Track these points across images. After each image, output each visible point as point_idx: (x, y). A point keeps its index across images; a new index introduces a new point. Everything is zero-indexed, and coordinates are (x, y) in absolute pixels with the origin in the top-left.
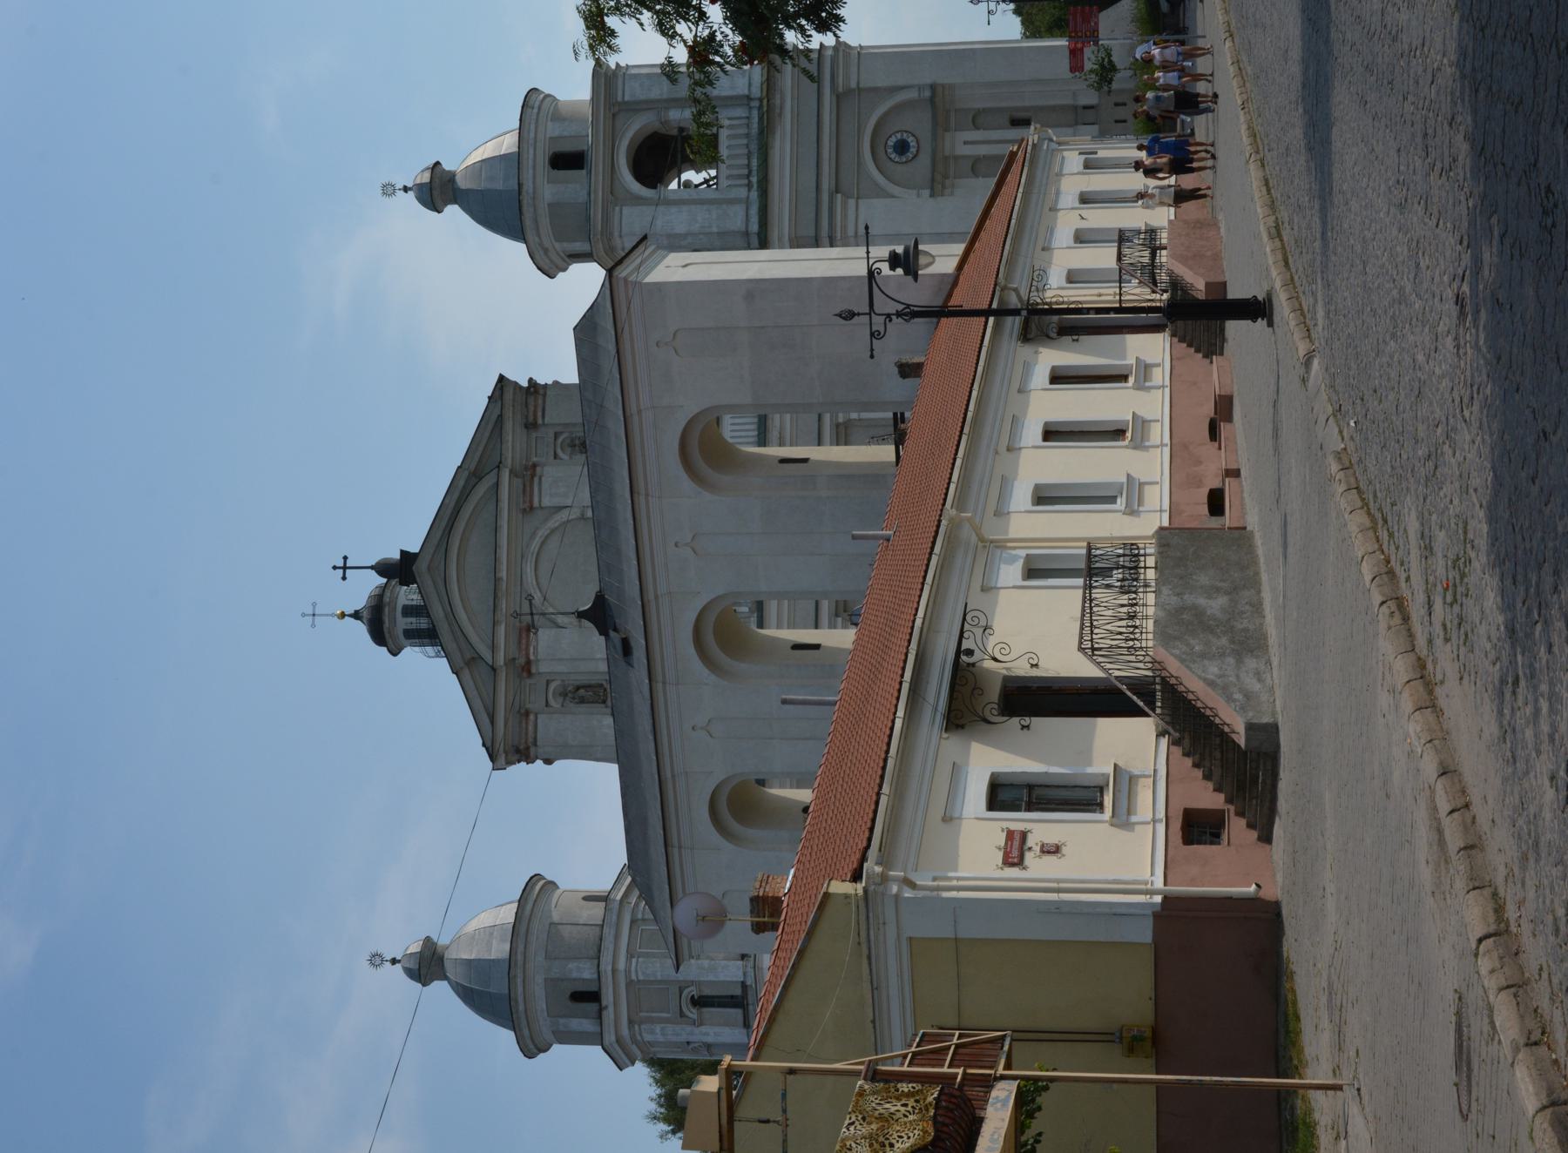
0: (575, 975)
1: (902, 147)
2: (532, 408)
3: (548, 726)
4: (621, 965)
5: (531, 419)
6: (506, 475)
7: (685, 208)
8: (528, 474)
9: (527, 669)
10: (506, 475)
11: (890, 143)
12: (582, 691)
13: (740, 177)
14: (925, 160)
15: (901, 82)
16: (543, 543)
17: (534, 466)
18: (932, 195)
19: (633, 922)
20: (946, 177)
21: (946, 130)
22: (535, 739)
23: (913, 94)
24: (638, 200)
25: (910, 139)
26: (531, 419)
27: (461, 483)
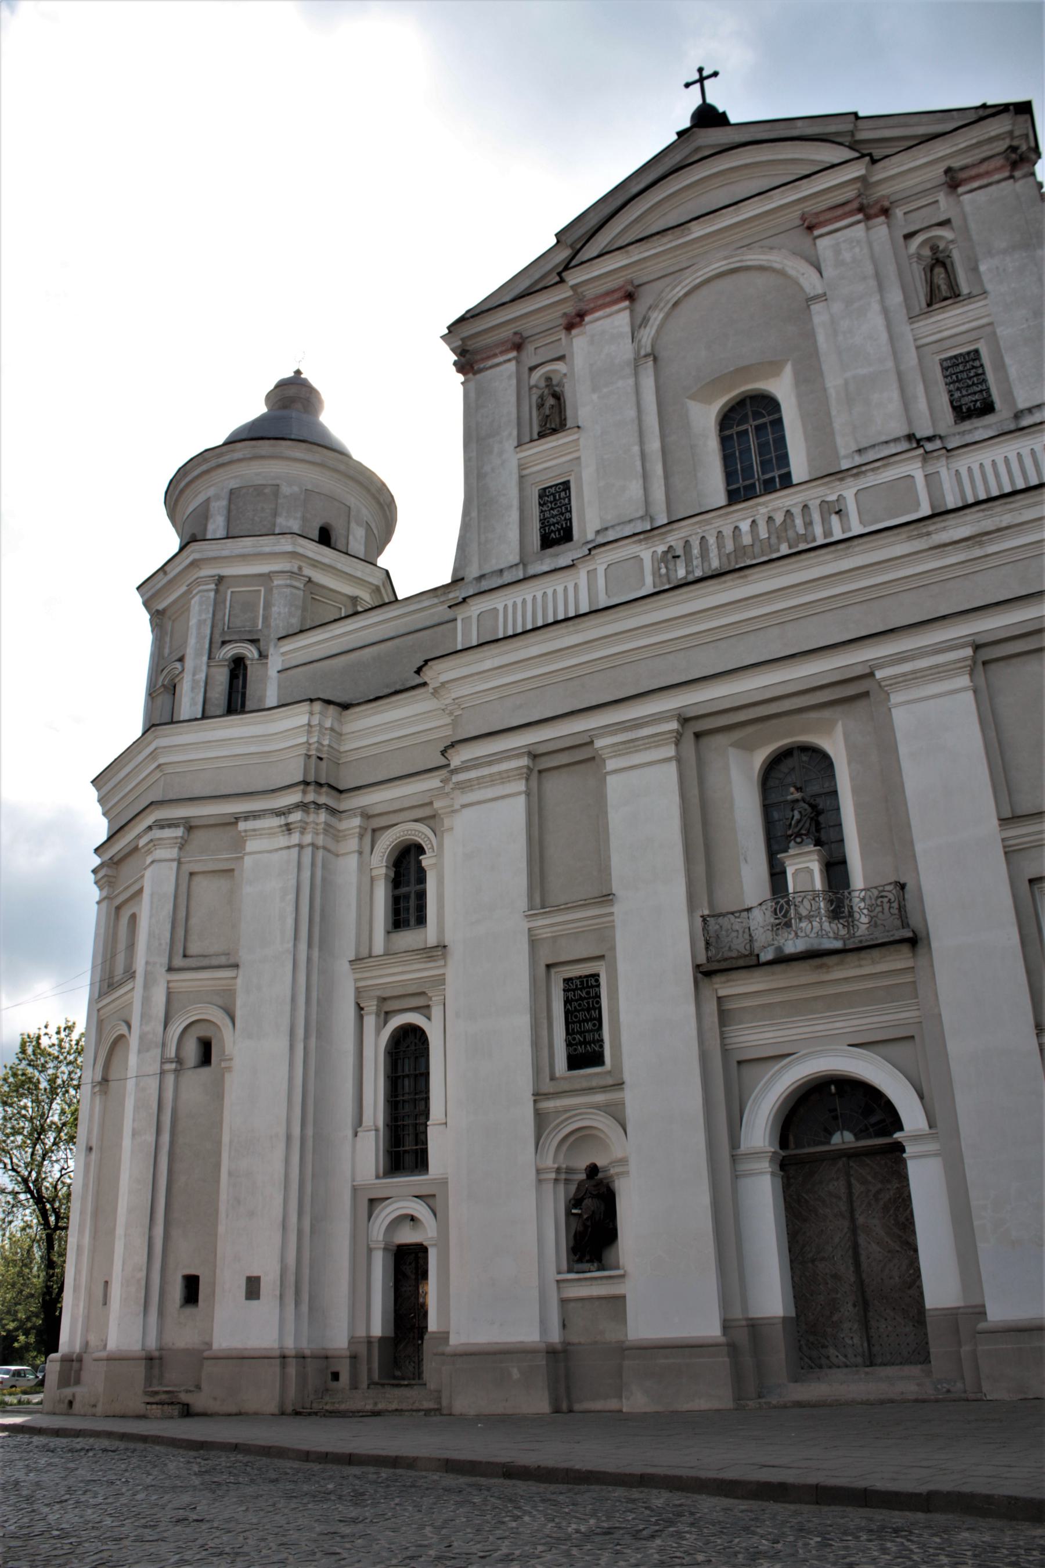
0: (211, 527)
3: (504, 375)
5: (963, 175)
8: (870, 209)
9: (574, 322)
10: (857, 170)
12: (551, 401)
16: (761, 268)
17: (885, 212)
19: (268, 577)
22: (480, 371)
26: (963, 175)
27: (832, 128)
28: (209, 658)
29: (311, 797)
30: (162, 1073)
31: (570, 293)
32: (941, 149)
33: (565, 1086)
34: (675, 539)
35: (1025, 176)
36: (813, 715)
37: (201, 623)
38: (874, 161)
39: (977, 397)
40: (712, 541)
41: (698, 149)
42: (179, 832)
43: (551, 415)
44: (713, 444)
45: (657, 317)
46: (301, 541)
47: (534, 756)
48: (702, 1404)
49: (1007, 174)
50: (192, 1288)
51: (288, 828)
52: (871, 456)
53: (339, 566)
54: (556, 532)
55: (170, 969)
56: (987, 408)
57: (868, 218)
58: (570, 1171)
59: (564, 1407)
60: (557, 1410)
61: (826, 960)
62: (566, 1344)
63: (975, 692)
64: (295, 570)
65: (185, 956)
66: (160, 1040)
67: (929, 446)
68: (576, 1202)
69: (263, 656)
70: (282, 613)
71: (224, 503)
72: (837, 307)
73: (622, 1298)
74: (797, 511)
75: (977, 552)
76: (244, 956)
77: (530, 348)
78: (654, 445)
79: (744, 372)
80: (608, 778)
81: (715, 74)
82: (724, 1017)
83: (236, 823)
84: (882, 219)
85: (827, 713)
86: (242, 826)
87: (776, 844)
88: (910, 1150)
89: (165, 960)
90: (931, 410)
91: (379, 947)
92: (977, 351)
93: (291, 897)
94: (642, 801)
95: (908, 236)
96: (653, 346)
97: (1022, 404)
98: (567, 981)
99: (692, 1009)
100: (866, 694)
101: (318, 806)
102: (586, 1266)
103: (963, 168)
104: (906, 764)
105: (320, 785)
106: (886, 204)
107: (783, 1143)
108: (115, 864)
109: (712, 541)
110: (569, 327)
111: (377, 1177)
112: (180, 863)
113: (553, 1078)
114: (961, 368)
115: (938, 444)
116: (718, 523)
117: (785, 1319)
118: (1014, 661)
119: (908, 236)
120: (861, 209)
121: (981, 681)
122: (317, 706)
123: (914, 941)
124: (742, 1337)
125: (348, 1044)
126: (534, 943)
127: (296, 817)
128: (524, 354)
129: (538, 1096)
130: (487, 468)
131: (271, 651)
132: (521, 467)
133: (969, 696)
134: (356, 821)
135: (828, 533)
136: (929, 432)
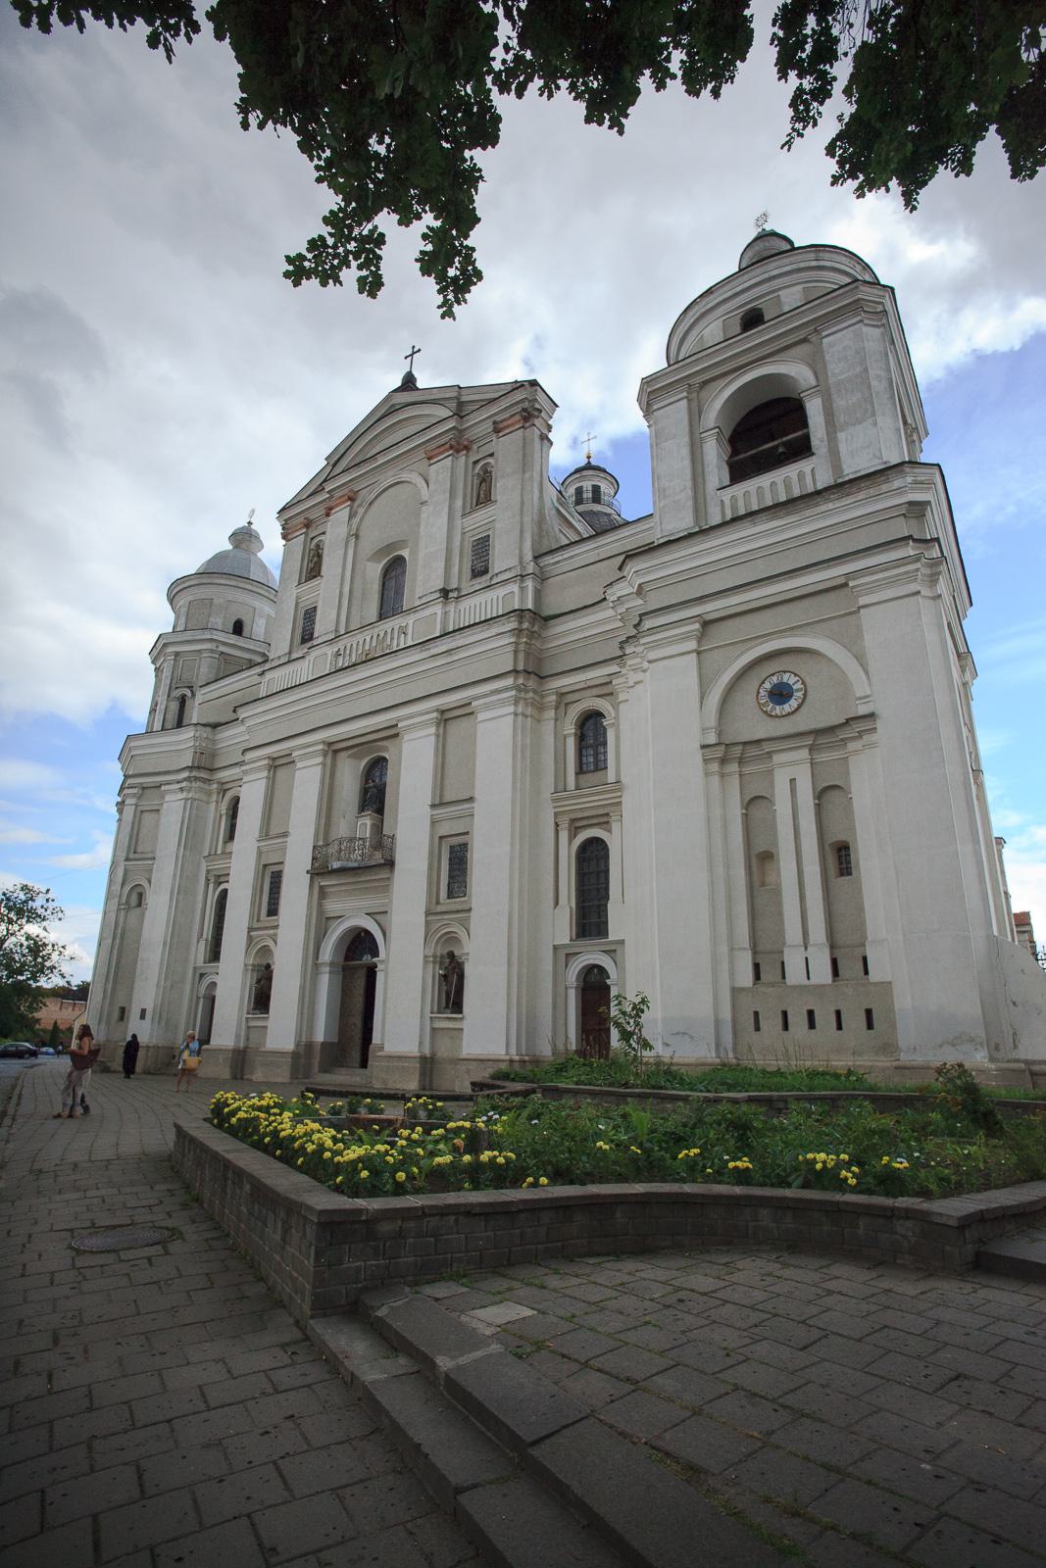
1: (780, 694)
2: (509, 422)
4: (170, 649)
6: (451, 424)
7: (687, 462)
8: (459, 445)
11: (786, 678)
13: (734, 507)
14: (763, 729)
15: (872, 667)
17: (467, 448)
18: (703, 747)
20: (741, 761)
21: (812, 749)
23: (861, 688)
24: (695, 414)
25: (793, 703)
26: (501, 426)
28: (169, 696)
29: (194, 774)
30: (119, 910)
31: (328, 495)
32: (494, 409)
33: (260, 925)
34: (340, 645)
35: (530, 426)
36: (379, 743)
37: (166, 677)
38: (462, 417)
39: (483, 564)
40: (355, 646)
41: (393, 406)
42: (135, 791)
43: (313, 569)
44: (376, 587)
45: (361, 511)
46: (215, 632)
47: (274, 759)
48: (279, 1080)
49: (521, 425)
50: (123, 1010)
51: (181, 789)
52: (424, 600)
53: (240, 644)
54: (307, 637)
55: (127, 859)
56: (486, 571)
57: (458, 451)
58: (259, 965)
59: (239, 1077)
60: (235, 1078)
61: (357, 871)
62: (246, 1048)
63: (438, 736)
64: (214, 648)
65: (135, 852)
66: (118, 894)
67: (451, 595)
68: (258, 981)
69: (193, 695)
70: (204, 670)
71: (186, 609)
72: (431, 508)
73: (266, 1027)
74: (389, 631)
75: (449, 660)
76: (158, 854)
77: (314, 525)
78: (346, 589)
79: (391, 547)
80: (298, 773)
81: (419, 350)
82: (323, 893)
83: (160, 786)
84: (464, 452)
85: (385, 743)
86: (163, 788)
87: (362, 808)
88: (380, 967)
89: (124, 854)
90: (460, 576)
91: (219, 852)
92: (489, 536)
93: (179, 825)
94: (306, 783)
95: (475, 463)
96: (357, 529)
97: (496, 572)
98: (273, 873)
99: (307, 891)
100: (396, 735)
101: (196, 779)
102: (256, 1012)
103: (502, 421)
104: (403, 772)
105: (199, 768)
106: (465, 443)
107: (347, 958)
108: (121, 806)
109: (355, 646)
110: (328, 515)
111: (205, 963)
112: (137, 806)
113: (258, 921)
114: (480, 546)
115: (455, 594)
116: (359, 636)
117: (323, 1043)
118: (458, 719)
119: (475, 463)
120: (451, 447)
121: (441, 731)
122: (199, 727)
123: (390, 864)
124: (302, 1050)
125: (200, 897)
126: (260, 853)
127: (184, 784)
128: (310, 530)
129: (250, 929)
130: (284, 598)
131: (198, 693)
132: (298, 598)
133: (433, 738)
134: (215, 786)
135: (398, 645)
136: (455, 586)
